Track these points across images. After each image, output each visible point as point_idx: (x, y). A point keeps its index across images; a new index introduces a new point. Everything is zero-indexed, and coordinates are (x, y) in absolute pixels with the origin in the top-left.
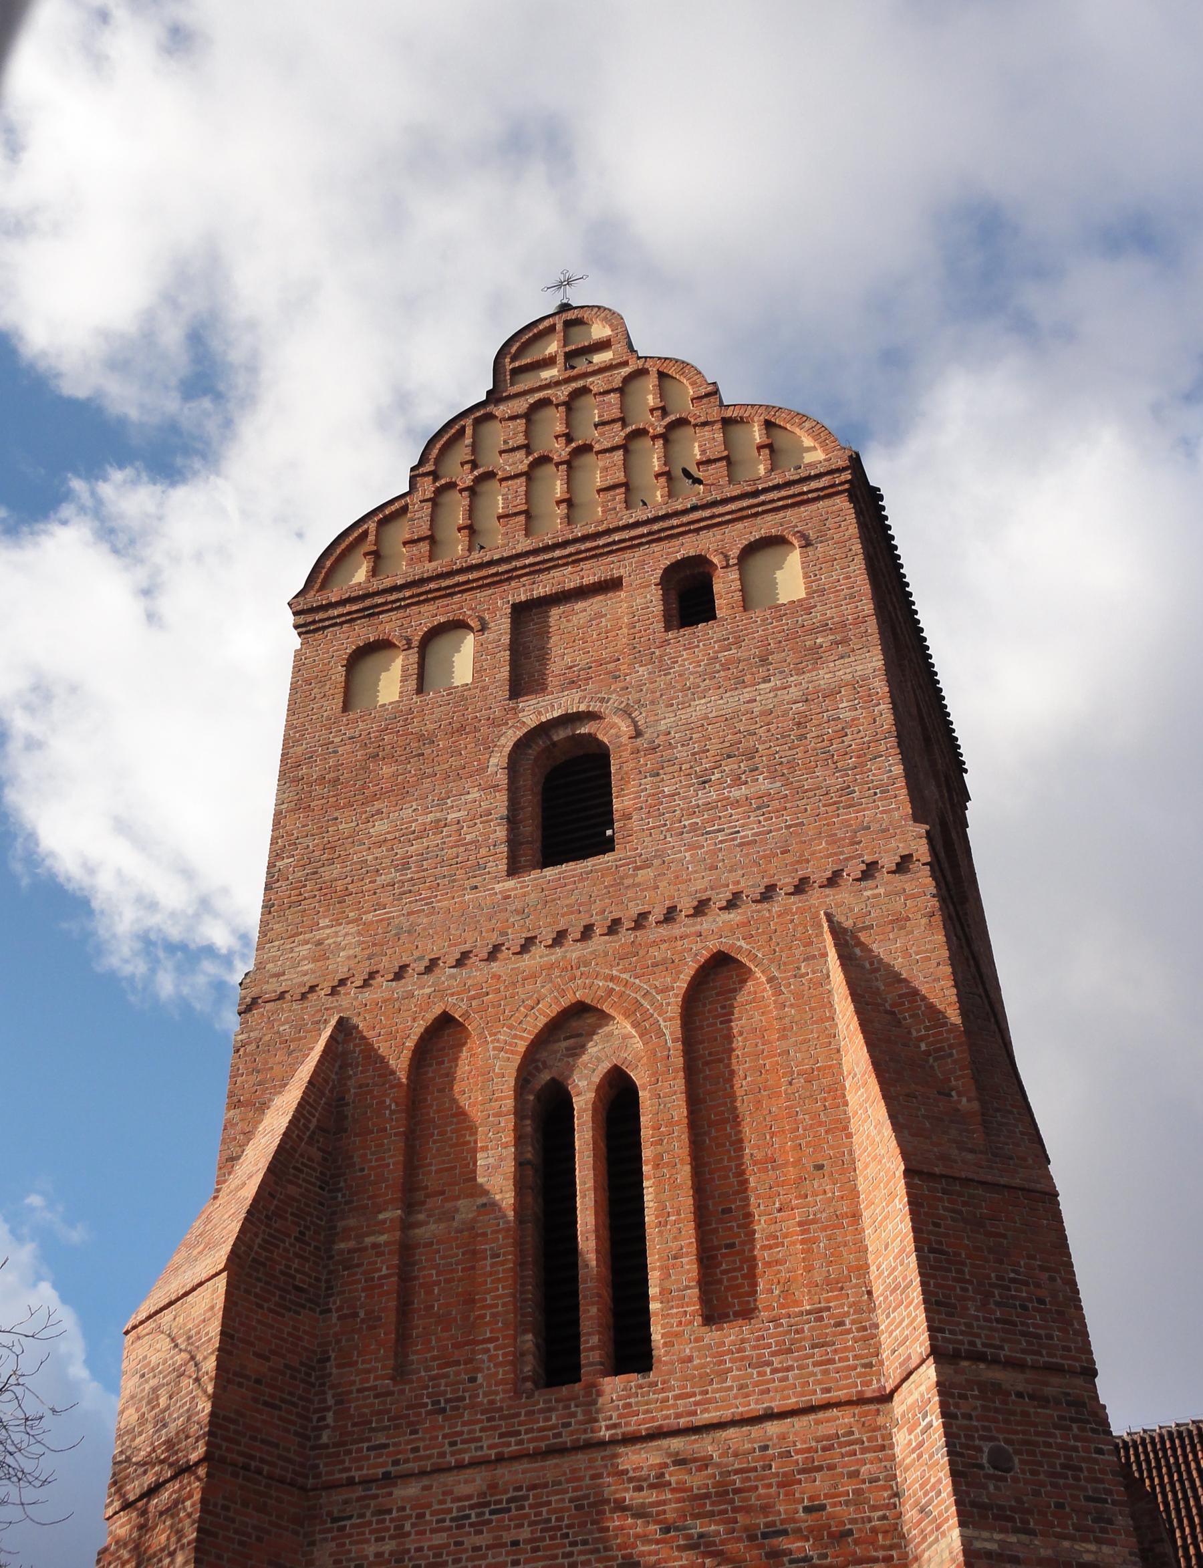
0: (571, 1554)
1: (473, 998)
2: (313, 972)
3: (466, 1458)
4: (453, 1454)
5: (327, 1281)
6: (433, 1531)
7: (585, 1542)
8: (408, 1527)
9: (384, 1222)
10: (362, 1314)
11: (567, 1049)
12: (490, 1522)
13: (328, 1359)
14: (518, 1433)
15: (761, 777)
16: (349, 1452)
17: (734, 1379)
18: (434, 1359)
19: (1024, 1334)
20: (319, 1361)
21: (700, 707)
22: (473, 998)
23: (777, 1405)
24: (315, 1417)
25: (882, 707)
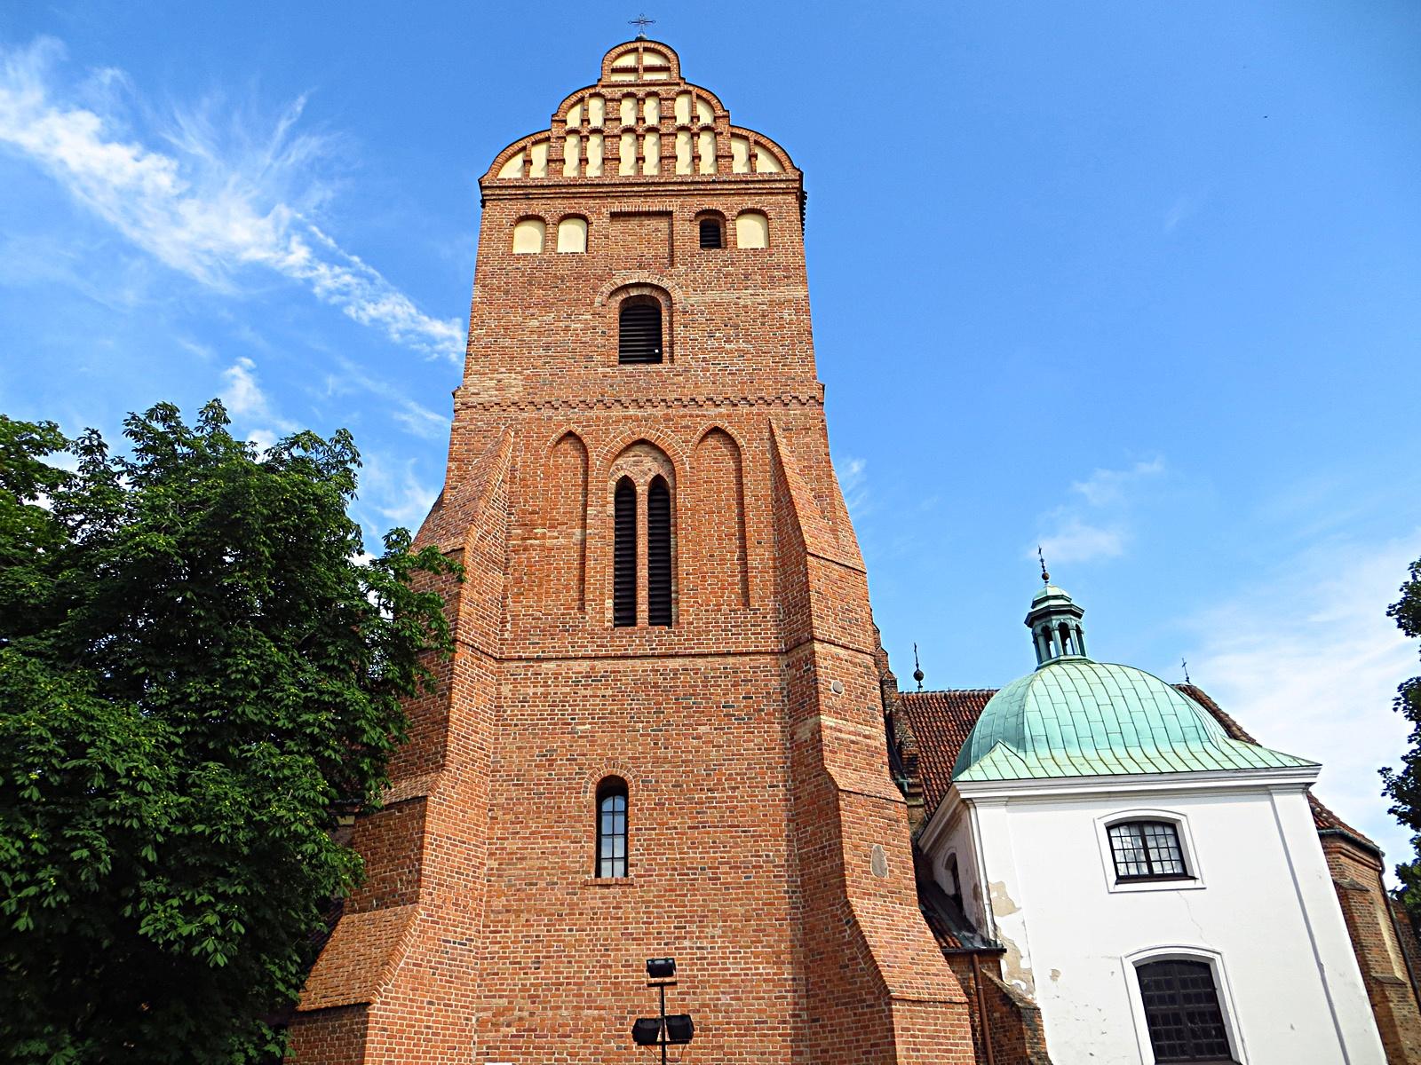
1: (585, 426)
3: (580, 654)
7: (638, 700)
9: (536, 534)
18: (562, 605)
21: (711, 296)
22: (585, 426)
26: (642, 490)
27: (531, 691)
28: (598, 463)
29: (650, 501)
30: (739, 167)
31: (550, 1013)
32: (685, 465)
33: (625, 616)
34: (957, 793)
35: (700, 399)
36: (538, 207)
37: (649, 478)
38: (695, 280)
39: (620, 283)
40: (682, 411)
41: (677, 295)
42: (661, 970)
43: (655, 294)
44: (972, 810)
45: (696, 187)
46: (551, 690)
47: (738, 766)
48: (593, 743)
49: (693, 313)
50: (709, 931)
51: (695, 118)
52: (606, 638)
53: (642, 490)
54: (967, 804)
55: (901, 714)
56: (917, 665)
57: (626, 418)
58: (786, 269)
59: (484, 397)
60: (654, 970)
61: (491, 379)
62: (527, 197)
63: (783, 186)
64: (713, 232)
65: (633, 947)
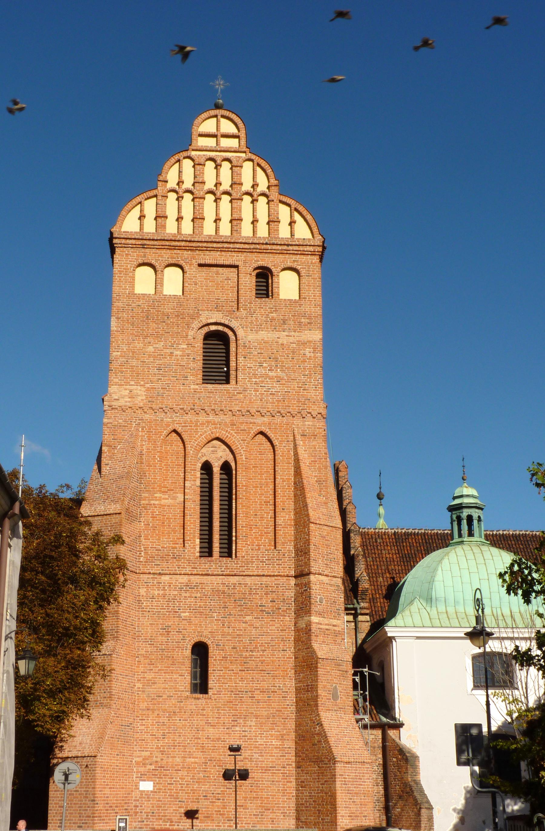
0: (210, 602)
2: (129, 402)
3: (183, 572)
4: (179, 571)
5: (140, 512)
6: (173, 590)
7: (214, 600)
8: (166, 588)
9: (156, 497)
10: (151, 525)
11: (212, 451)
12: (189, 590)
13: (141, 536)
14: (197, 568)
15: (279, 370)
16: (149, 565)
17: (255, 564)
18: (171, 541)
19: (330, 568)
20: (139, 536)
21: (263, 335)
23: (265, 573)
24: (138, 553)
25: (319, 354)
26: (216, 470)
27: (156, 592)
28: (191, 452)
30: (284, 232)
31: (170, 760)
32: (242, 457)
33: (207, 551)
35: (253, 411)
37: (221, 463)
38: (252, 322)
39: (205, 322)
40: (242, 419)
41: (240, 333)
42: (235, 749)
43: (226, 330)
45: (253, 246)
46: (167, 592)
47: (266, 639)
48: (190, 623)
49: (249, 348)
50: (249, 723)
51: (255, 186)
52: (197, 563)
54: (391, 639)
55: (361, 557)
56: (380, 488)
57: (208, 422)
58: (310, 318)
59: (122, 402)
60: (232, 749)
61: (126, 389)
62: (143, 246)
63: (311, 249)
64: (264, 278)
65: (211, 730)
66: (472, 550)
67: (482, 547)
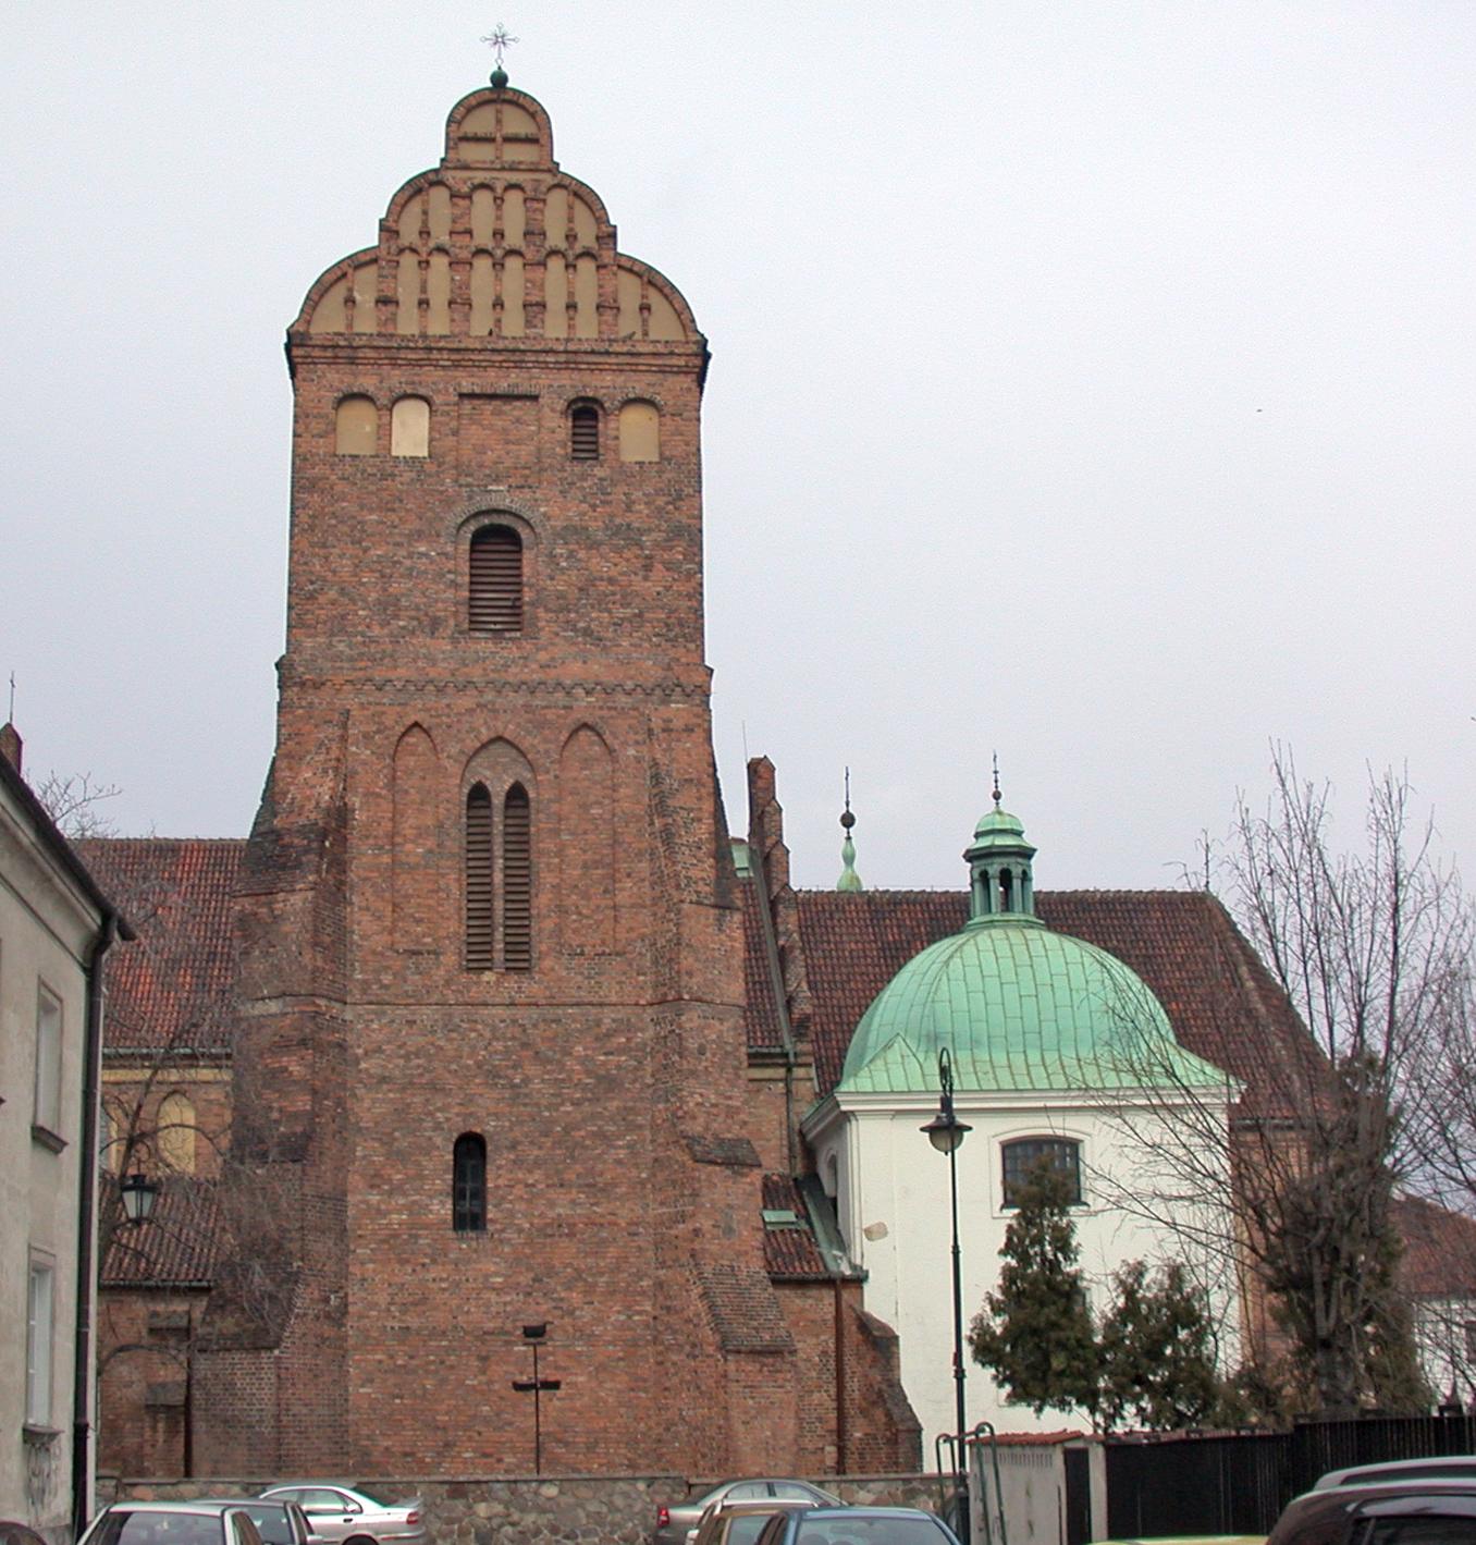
26: (498, 801)
29: (507, 806)
33: (477, 957)
34: (837, 1105)
36: (367, 383)
44: (854, 1122)
45: (572, 358)
53: (498, 801)
54: (847, 1116)
55: (797, 952)
56: (847, 804)
66: (1008, 938)
67: (1026, 931)
